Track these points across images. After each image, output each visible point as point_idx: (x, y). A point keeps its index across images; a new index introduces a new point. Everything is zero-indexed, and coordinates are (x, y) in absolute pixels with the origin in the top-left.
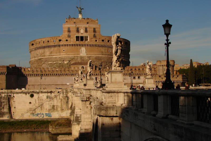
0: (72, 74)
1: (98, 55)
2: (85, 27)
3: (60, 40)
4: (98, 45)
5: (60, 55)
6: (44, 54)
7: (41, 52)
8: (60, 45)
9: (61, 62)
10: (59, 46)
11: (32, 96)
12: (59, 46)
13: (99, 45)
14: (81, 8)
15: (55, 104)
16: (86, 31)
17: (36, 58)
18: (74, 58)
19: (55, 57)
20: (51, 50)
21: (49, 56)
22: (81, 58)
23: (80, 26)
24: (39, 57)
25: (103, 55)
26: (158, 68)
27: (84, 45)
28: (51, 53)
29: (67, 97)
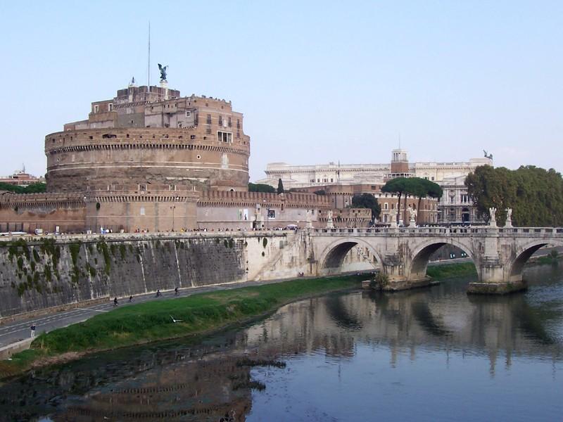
3: (193, 137)
5: (191, 165)
6: (151, 160)
7: (144, 156)
9: (194, 179)
10: (191, 147)
11: (265, 243)
12: (191, 147)
15: (294, 255)
16: (230, 125)
17: (121, 166)
18: (214, 173)
19: (181, 169)
20: (171, 153)
21: (167, 164)
22: (223, 172)
29: (305, 242)
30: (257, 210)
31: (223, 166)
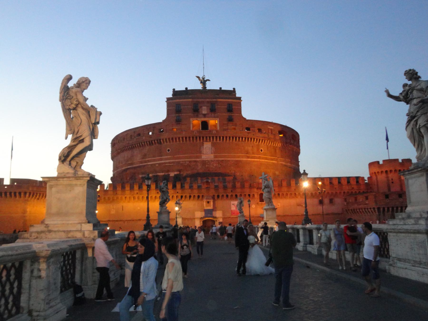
0: (182, 197)
1: (239, 158)
2: (211, 101)
4: (239, 138)
5: (161, 160)
8: (160, 140)
13: (241, 138)
14: (205, 79)
17: (118, 170)
18: (190, 166)
19: (151, 165)
21: (141, 162)
22: (204, 163)
23: (200, 100)
24: (122, 167)
25: (248, 157)
26: (374, 178)
27: (210, 137)
28: (145, 156)
30: (205, 203)
31: (203, 157)
